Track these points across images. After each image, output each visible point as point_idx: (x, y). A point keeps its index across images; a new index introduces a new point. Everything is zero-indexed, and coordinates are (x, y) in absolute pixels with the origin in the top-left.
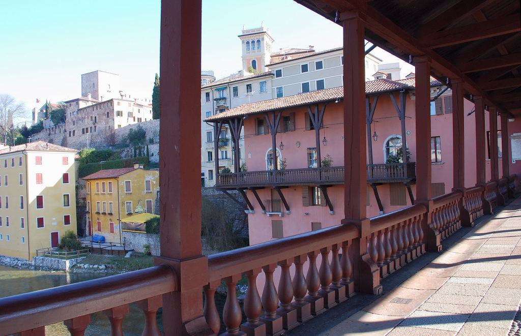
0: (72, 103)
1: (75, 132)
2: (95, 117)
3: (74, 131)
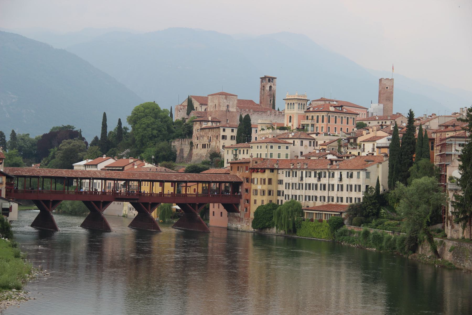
0: (197, 122)
1: (198, 145)
2: (210, 137)
3: (197, 145)
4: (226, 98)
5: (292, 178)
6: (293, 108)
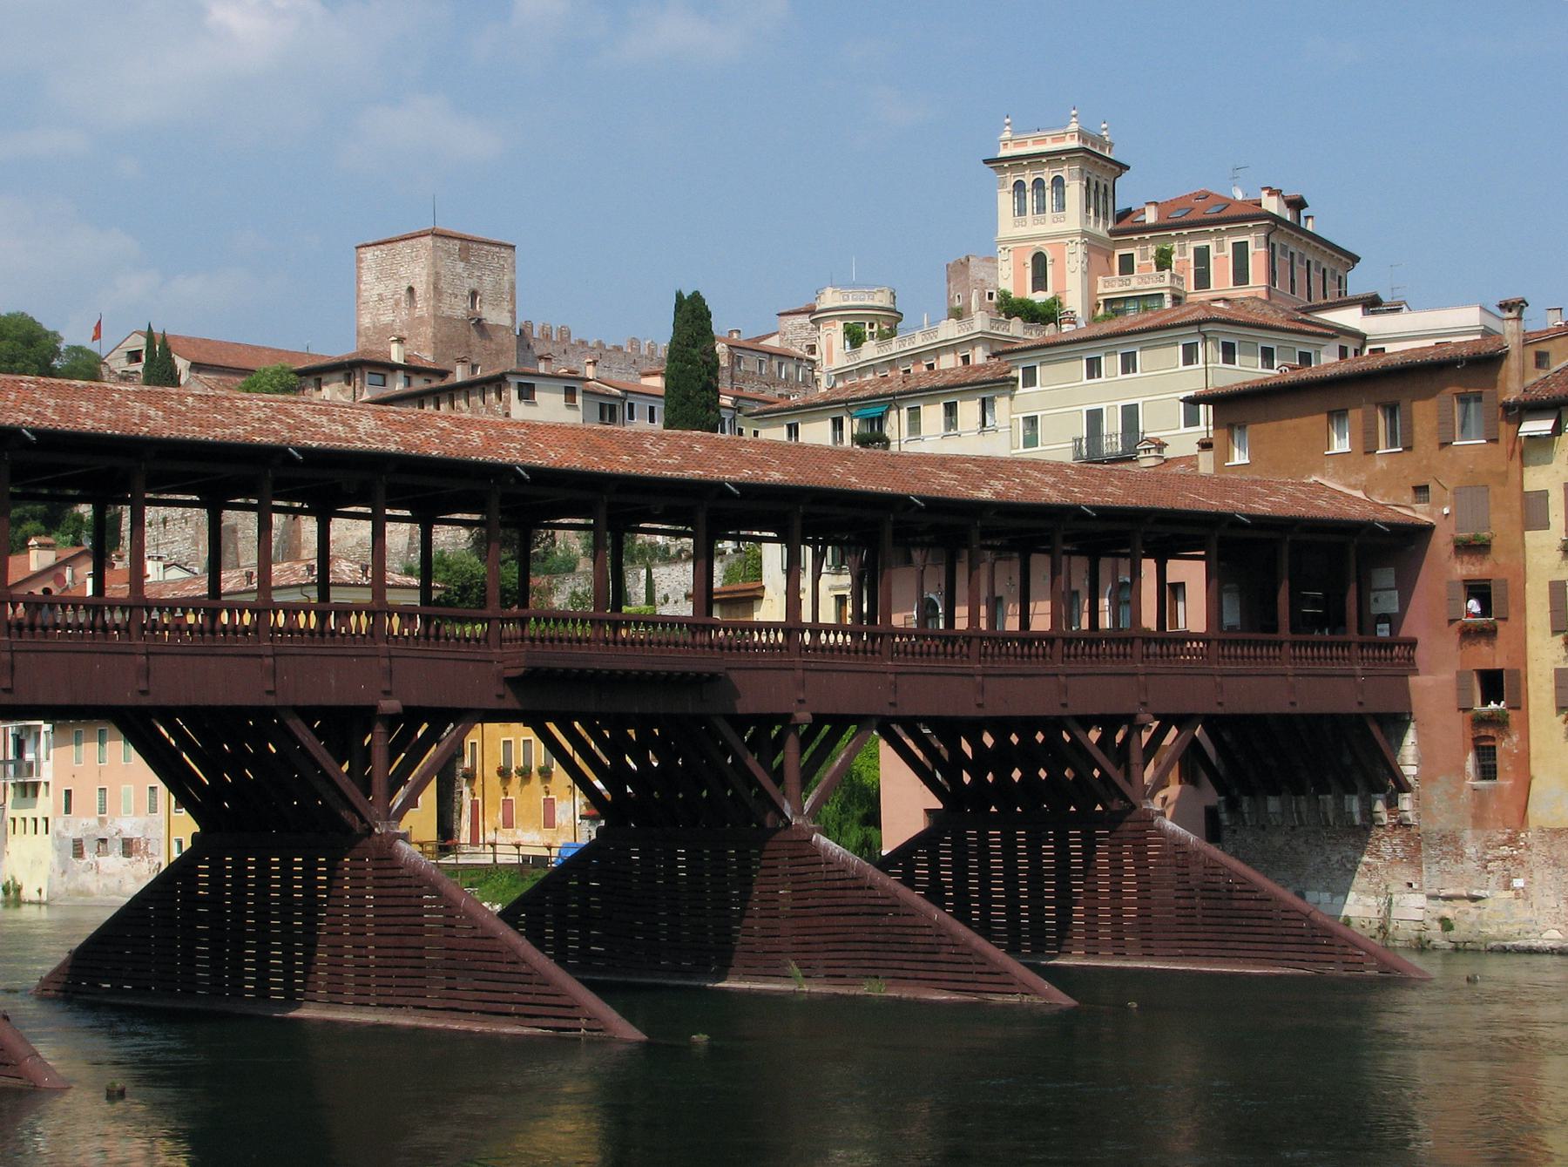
0: (325, 378)
4: (464, 256)
6: (1061, 206)
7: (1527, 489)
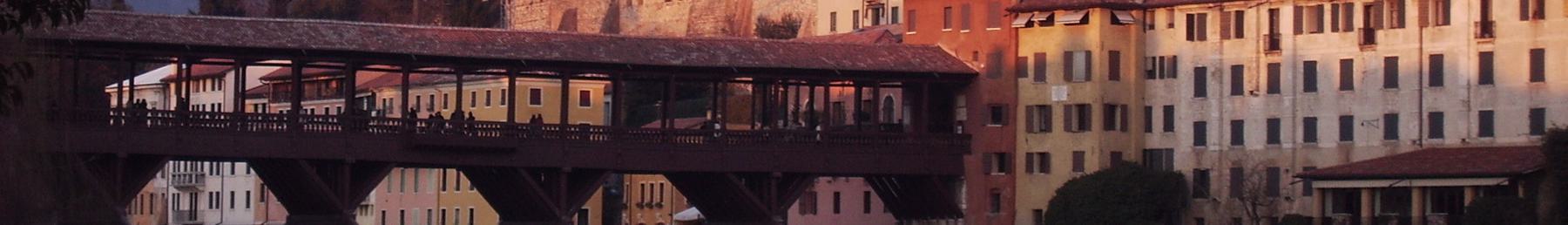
5: (1221, 43)
7: (1020, 55)
